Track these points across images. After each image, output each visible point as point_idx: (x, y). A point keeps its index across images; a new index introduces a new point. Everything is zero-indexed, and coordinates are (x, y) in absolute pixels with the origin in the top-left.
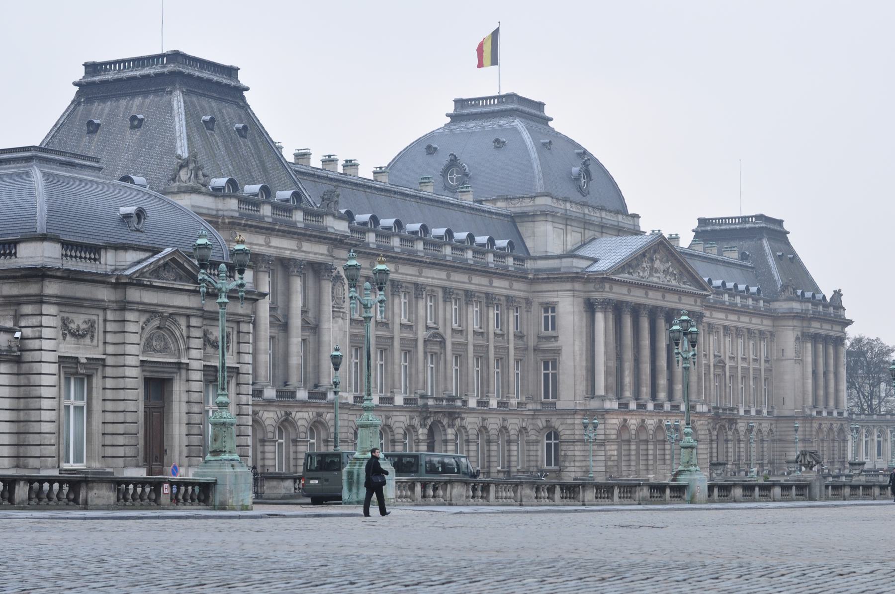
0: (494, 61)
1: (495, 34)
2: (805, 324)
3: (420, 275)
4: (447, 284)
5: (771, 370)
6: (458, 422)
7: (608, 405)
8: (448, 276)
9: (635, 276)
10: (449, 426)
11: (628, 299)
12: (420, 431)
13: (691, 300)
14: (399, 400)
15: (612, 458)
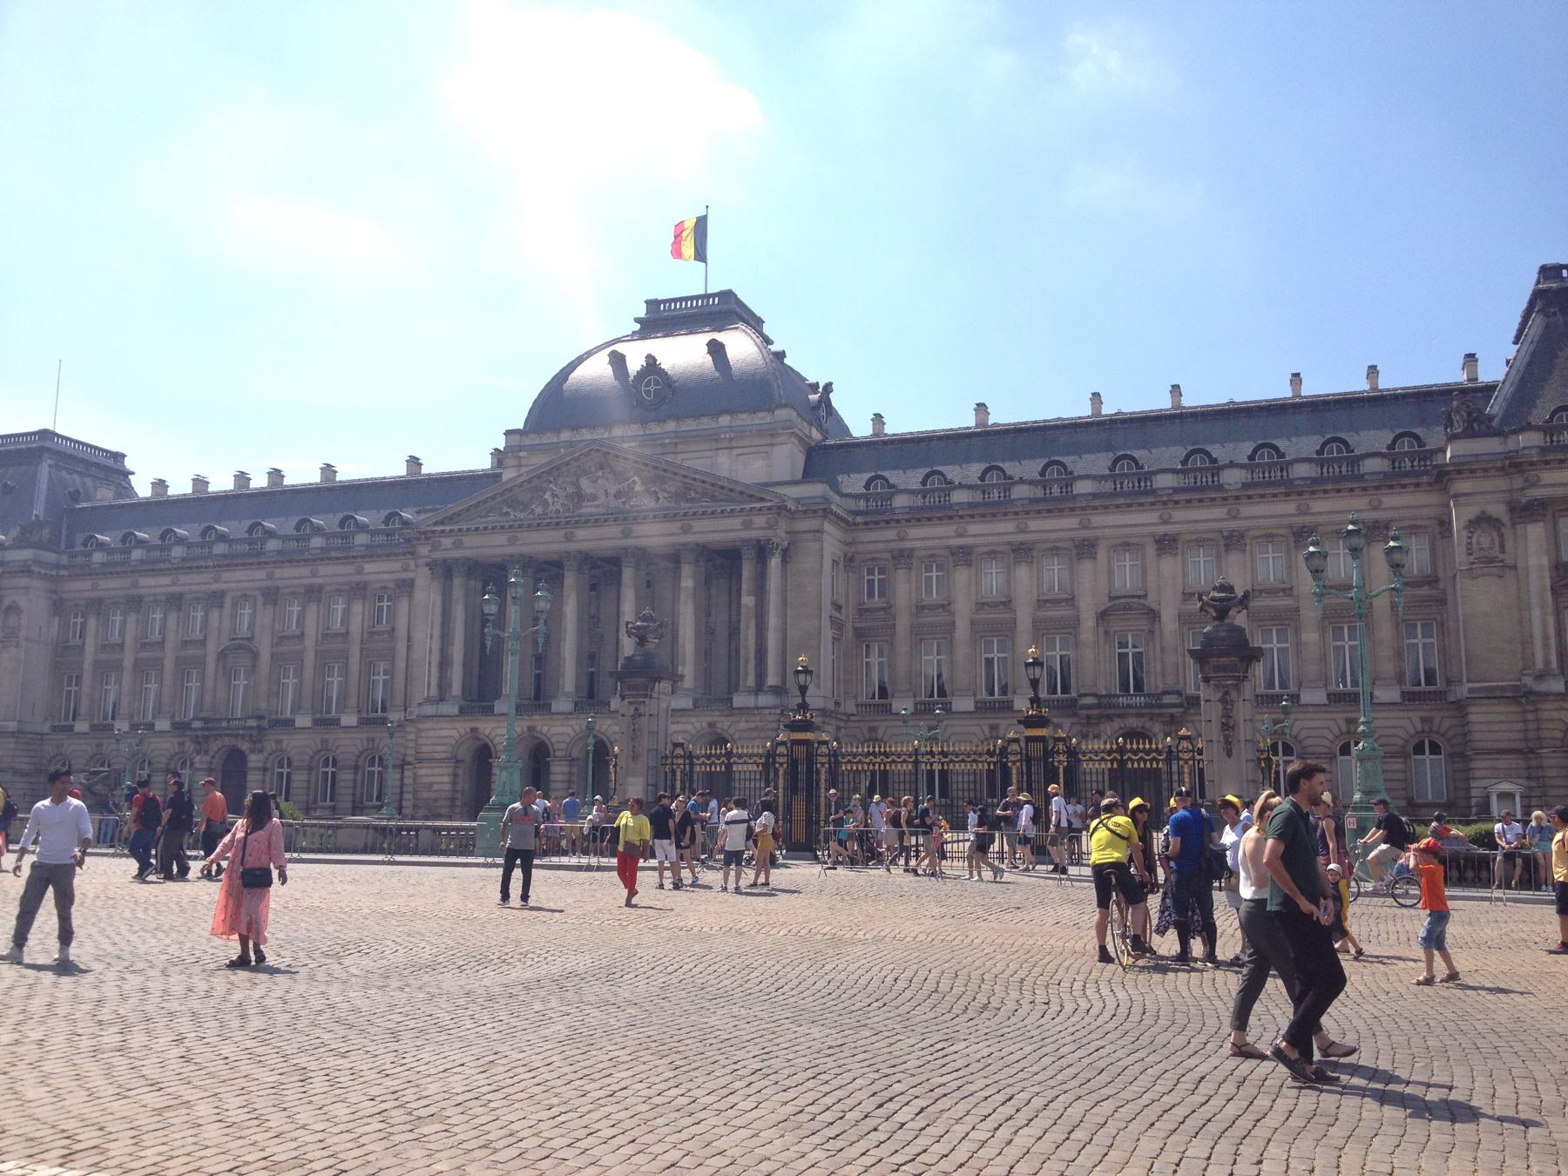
0: (701, 255)
1: (701, 224)
2: (1518, 482)
3: (217, 580)
4: (269, 583)
5: (1442, 602)
6: (270, 745)
7: (429, 710)
8: (270, 577)
9: (522, 516)
10: (252, 751)
11: (510, 550)
12: (198, 759)
13: (736, 523)
14: (163, 725)
15: (435, 787)
